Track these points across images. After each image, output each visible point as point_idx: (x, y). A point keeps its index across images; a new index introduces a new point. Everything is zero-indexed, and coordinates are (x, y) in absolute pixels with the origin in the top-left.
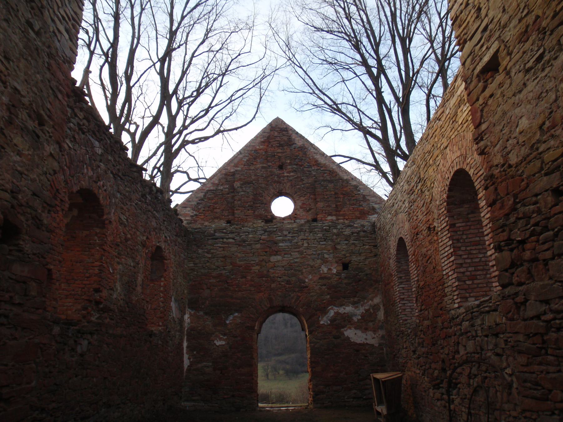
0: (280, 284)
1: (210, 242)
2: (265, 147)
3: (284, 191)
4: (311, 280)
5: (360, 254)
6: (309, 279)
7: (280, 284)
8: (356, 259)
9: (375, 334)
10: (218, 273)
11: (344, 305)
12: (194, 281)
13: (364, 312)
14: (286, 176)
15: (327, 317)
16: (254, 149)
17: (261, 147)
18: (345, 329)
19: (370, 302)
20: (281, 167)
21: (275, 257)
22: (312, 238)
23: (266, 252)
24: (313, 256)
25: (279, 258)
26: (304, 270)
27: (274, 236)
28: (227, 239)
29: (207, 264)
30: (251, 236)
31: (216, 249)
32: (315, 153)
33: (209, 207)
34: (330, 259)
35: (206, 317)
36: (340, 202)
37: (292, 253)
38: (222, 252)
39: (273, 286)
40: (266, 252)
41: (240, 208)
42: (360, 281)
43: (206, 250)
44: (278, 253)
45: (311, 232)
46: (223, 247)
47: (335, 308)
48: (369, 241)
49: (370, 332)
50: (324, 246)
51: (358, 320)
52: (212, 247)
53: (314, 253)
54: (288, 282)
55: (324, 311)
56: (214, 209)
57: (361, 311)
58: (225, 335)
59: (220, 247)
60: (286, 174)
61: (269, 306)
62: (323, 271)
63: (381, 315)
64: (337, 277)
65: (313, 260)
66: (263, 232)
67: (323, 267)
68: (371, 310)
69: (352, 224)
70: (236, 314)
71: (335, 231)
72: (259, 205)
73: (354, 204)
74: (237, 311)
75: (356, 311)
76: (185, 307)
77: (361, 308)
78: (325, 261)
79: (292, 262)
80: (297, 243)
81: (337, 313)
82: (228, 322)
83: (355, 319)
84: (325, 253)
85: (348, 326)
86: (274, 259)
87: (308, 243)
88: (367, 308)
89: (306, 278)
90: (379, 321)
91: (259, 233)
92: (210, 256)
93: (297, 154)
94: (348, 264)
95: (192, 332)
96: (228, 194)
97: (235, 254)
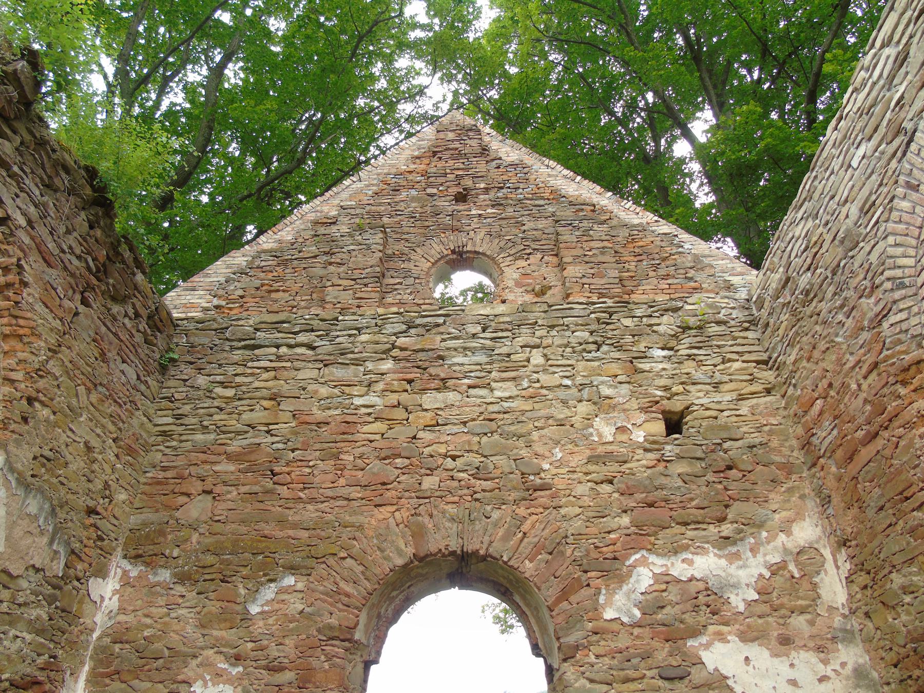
0: (452, 478)
1: (238, 355)
2: (423, 167)
3: (469, 248)
4: (560, 464)
5: (717, 386)
6: (554, 460)
7: (452, 478)
8: (704, 401)
9: (825, 662)
10: (245, 442)
11: (686, 548)
12: (165, 469)
13: (767, 574)
14: (474, 216)
15: (628, 595)
16: (394, 171)
17: (412, 167)
18: (704, 639)
19: (782, 537)
20: (461, 198)
21: (440, 396)
22: (558, 341)
23: (410, 382)
24: (561, 394)
25: (452, 397)
26: (535, 435)
27: (439, 338)
28: (290, 346)
29: (216, 417)
30: (364, 338)
31: (252, 374)
32: (549, 176)
33: (257, 289)
34: (621, 400)
35: (180, 589)
36: (628, 271)
37: (494, 385)
38: (270, 384)
39: (429, 483)
40: (410, 382)
41: (340, 282)
42: (729, 468)
43: (218, 378)
44: (450, 383)
45: (552, 327)
46: (274, 369)
47: (652, 558)
48: (740, 349)
49: (803, 654)
50: (596, 364)
51: (749, 604)
52: (240, 370)
53: (568, 382)
54: (479, 473)
55: (612, 569)
56: (270, 292)
57: (755, 572)
58: (238, 659)
59: (266, 369)
60: (474, 212)
61: (410, 551)
62: (600, 435)
63: (834, 587)
64: (650, 455)
65: (564, 402)
66: (404, 327)
67: (598, 422)
68: (792, 567)
69: (680, 304)
70: (290, 581)
71: (628, 322)
72: (398, 280)
73: (667, 276)
74: (292, 569)
75: (732, 570)
76: (107, 553)
77: (752, 561)
78: (602, 404)
79: (495, 408)
80: (509, 355)
81: (666, 580)
82: (254, 609)
83: (737, 601)
84: (603, 383)
85: (711, 629)
86: (431, 400)
87: (545, 355)
88: (775, 558)
89: (544, 457)
90: (831, 609)
91: (389, 329)
92: (230, 393)
93: (505, 177)
94: (682, 414)
95: (117, 647)
96: (315, 257)
97: (310, 388)
